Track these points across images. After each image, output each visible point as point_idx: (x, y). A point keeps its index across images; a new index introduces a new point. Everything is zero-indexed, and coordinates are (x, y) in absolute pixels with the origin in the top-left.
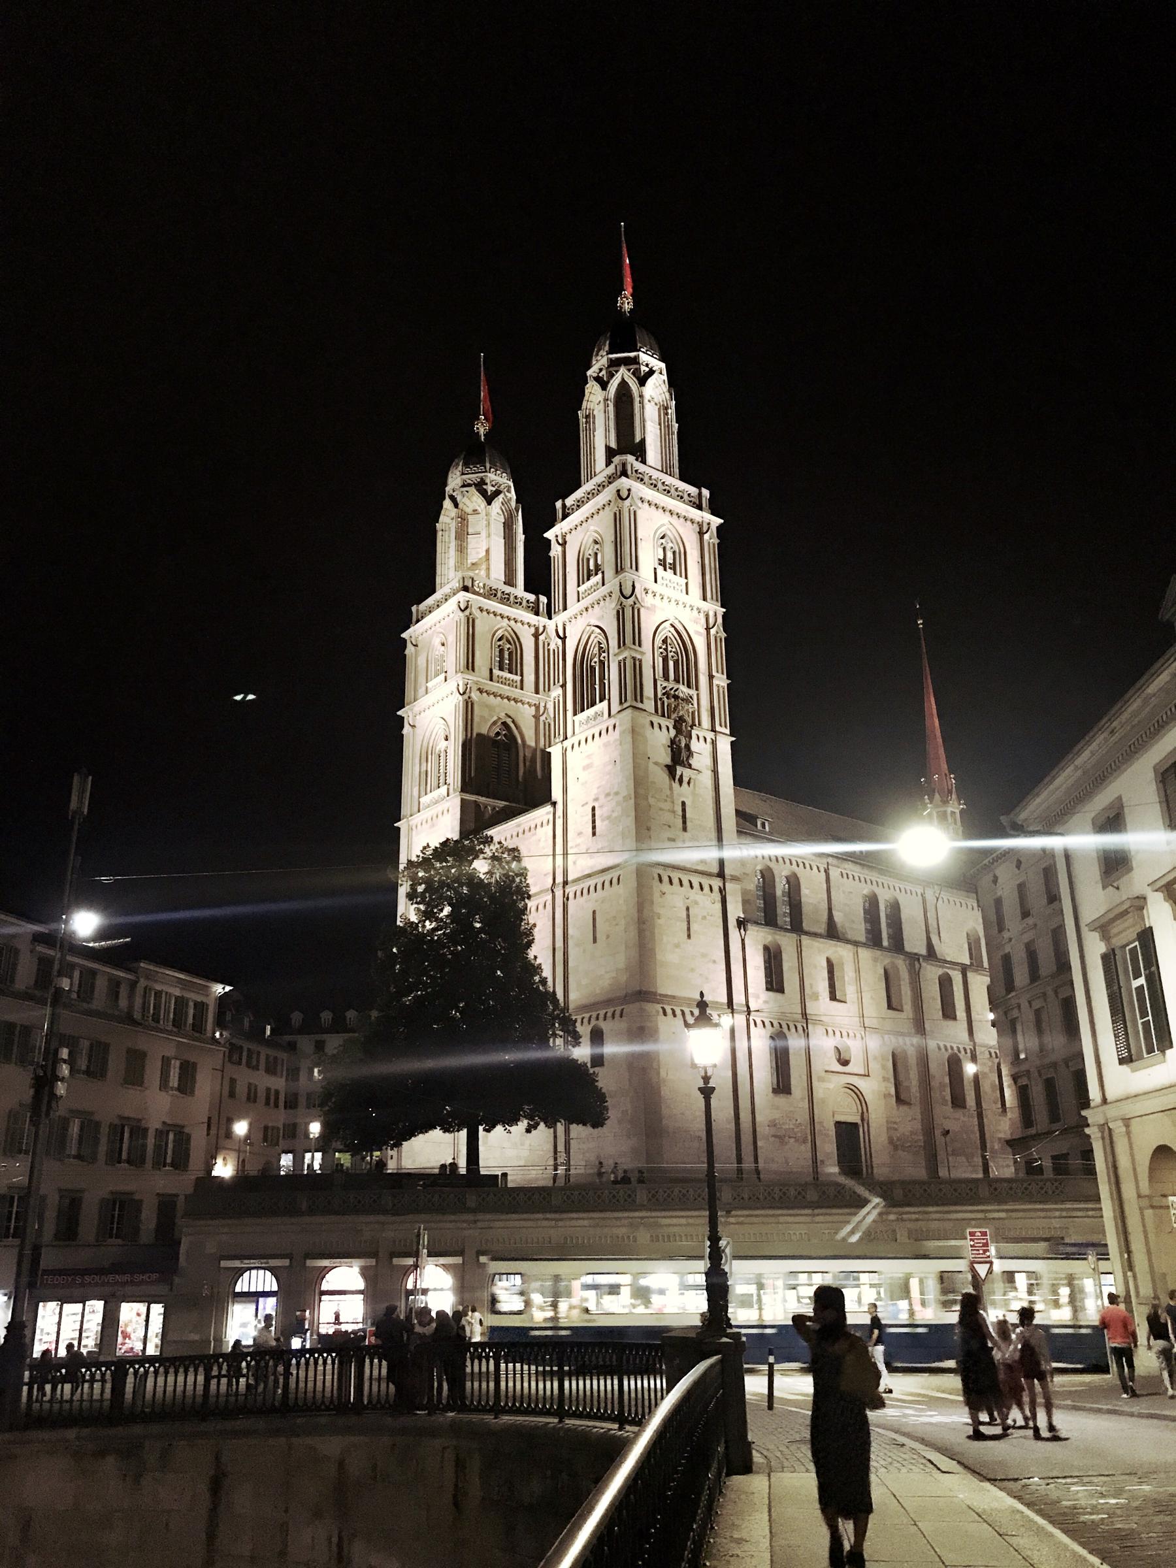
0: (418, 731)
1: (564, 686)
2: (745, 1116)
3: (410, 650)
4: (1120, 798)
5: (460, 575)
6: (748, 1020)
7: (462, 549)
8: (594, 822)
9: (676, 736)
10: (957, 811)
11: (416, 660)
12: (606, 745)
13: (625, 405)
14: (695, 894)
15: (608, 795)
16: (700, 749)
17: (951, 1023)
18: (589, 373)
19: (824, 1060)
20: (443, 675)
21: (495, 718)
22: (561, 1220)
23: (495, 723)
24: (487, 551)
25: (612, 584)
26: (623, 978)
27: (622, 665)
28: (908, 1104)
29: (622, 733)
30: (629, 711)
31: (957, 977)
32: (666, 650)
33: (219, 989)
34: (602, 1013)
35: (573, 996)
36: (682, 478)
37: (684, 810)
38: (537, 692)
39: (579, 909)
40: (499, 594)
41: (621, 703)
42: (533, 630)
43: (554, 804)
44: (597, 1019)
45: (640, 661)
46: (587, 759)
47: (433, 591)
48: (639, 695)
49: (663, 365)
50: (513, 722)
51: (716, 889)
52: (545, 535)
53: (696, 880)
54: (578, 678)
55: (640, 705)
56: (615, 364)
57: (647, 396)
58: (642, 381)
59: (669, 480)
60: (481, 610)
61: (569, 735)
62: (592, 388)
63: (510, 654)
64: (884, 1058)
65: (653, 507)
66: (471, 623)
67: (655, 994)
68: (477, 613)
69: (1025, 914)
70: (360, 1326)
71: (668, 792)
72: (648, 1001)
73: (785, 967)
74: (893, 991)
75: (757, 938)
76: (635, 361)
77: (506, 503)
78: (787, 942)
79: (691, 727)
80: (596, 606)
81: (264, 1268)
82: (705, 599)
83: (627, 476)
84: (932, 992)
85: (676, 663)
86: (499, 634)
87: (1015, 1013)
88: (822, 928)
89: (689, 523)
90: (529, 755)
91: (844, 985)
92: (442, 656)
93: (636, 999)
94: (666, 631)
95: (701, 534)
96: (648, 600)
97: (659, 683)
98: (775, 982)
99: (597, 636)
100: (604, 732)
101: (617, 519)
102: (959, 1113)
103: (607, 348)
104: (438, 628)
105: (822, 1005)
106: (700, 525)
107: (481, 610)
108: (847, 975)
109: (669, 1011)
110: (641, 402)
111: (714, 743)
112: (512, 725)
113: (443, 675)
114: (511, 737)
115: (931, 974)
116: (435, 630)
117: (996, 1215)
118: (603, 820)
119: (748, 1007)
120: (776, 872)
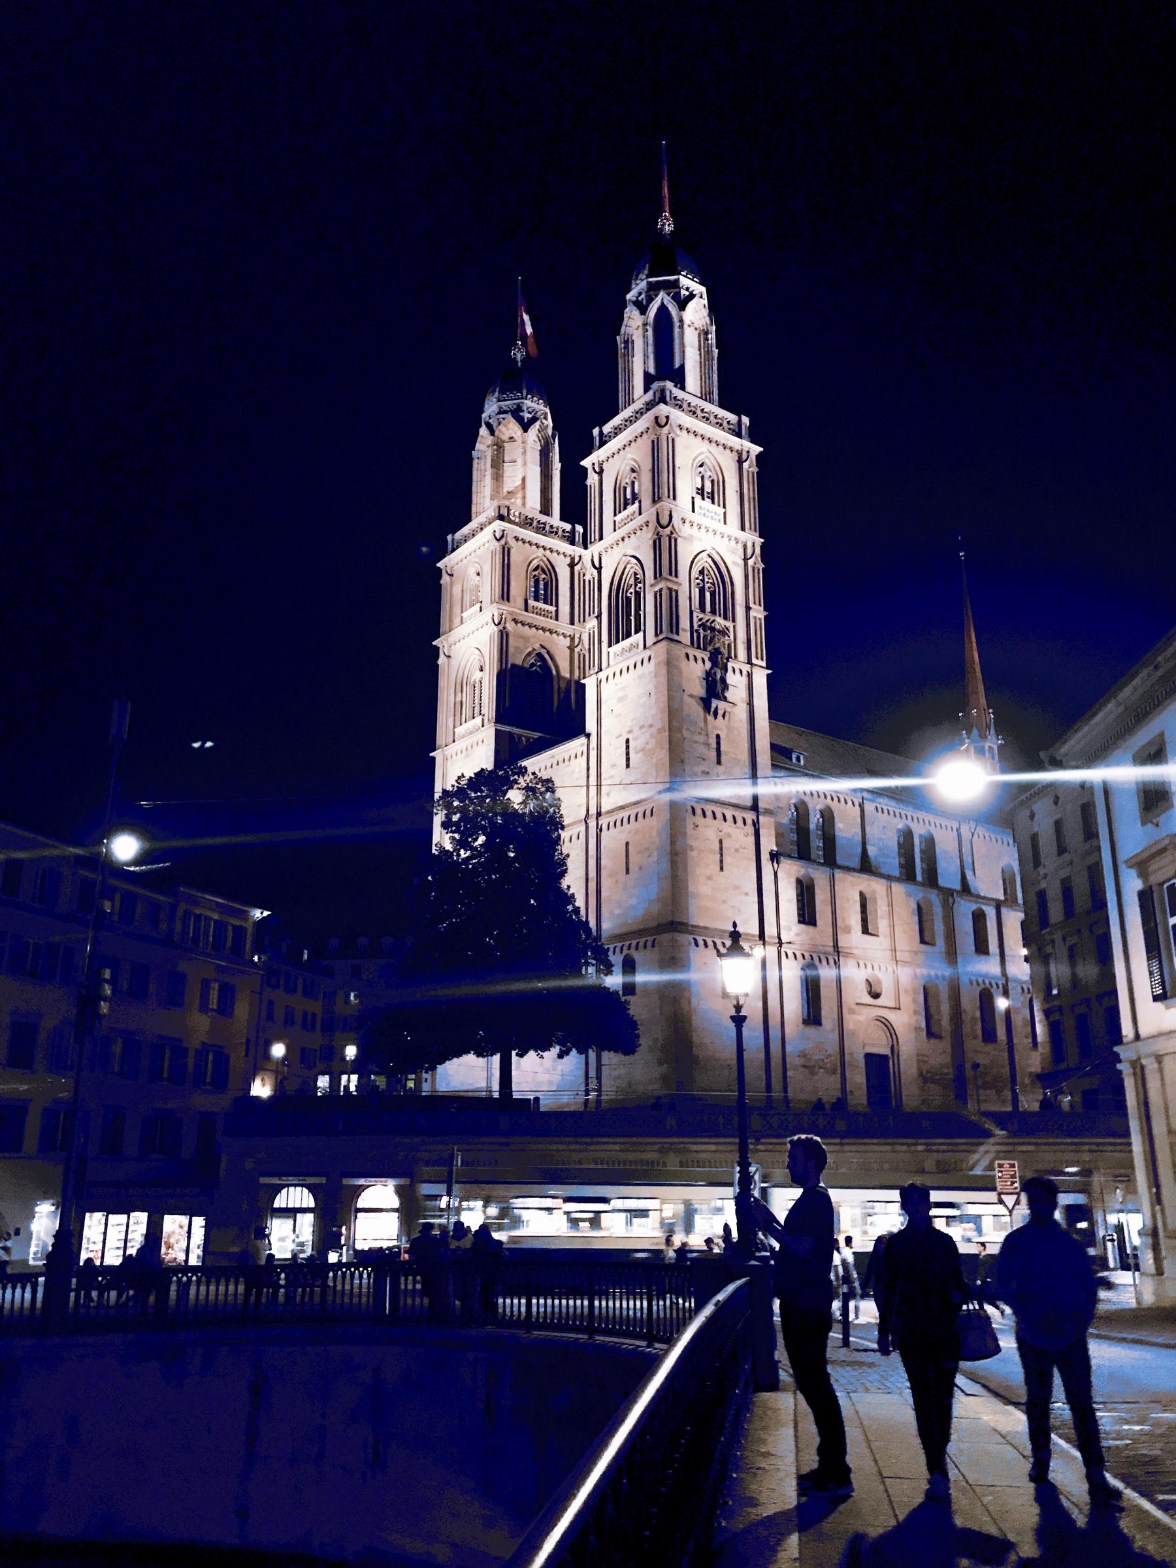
0: (453, 661)
1: (599, 617)
2: (775, 1046)
3: (445, 579)
4: (1162, 735)
5: (496, 503)
6: (779, 953)
7: (498, 477)
8: (628, 754)
9: (712, 668)
10: (995, 747)
11: (452, 590)
12: (641, 677)
14: (728, 827)
15: (642, 727)
17: (983, 957)
18: (628, 297)
19: (856, 993)
20: (477, 606)
21: (530, 649)
22: (591, 1144)
23: (529, 654)
24: (524, 479)
25: (649, 513)
26: (656, 908)
27: (658, 596)
28: (939, 1037)
29: (658, 664)
30: (664, 644)
31: (990, 912)
32: (703, 580)
33: (258, 914)
34: (634, 943)
35: (604, 926)
36: (722, 405)
37: (718, 743)
38: (572, 623)
39: (613, 840)
40: (535, 523)
41: (656, 635)
42: (568, 560)
43: (588, 736)
44: (629, 947)
45: (677, 592)
46: (623, 691)
47: (468, 520)
48: (674, 626)
49: (703, 289)
50: (548, 652)
51: (749, 822)
52: (582, 463)
53: (729, 813)
55: (676, 637)
56: (653, 289)
57: (687, 321)
58: (682, 304)
59: (708, 407)
60: (517, 539)
61: (604, 666)
63: (546, 585)
64: (915, 991)
65: (692, 435)
66: (506, 552)
67: (685, 925)
68: (512, 542)
69: (1062, 850)
70: (395, 1243)
71: (702, 725)
72: (681, 932)
73: (818, 902)
74: (926, 925)
75: (789, 872)
76: (676, 284)
77: (543, 429)
78: (820, 877)
79: (728, 660)
80: (632, 536)
81: (302, 1186)
82: (743, 529)
83: (666, 403)
84: (965, 926)
85: (713, 594)
86: (535, 564)
87: (1049, 949)
88: (856, 862)
89: (728, 451)
90: (563, 685)
91: (876, 918)
92: (477, 586)
93: (668, 929)
94: (703, 561)
95: (740, 462)
96: (685, 530)
97: (695, 615)
98: (807, 916)
99: (633, 566)
100: (639, 664)
101: (655, 447)
102: (989, 1048)
103: (646, 272)
104: (473, 558)
105: (853, 938)
106: (740, 453)
107: (517, 539)
108: (880, 908)
109: (701, 943)
110: (681, 327)
111: (750, 675)
112: (547, 656)
113: (477, 606)
114: (545, 667)
115: (964, 910)
116: (471, 560)
117: (1024, 1148)
118: (637, 753)
119: (780, 939)
120: (810, 806)
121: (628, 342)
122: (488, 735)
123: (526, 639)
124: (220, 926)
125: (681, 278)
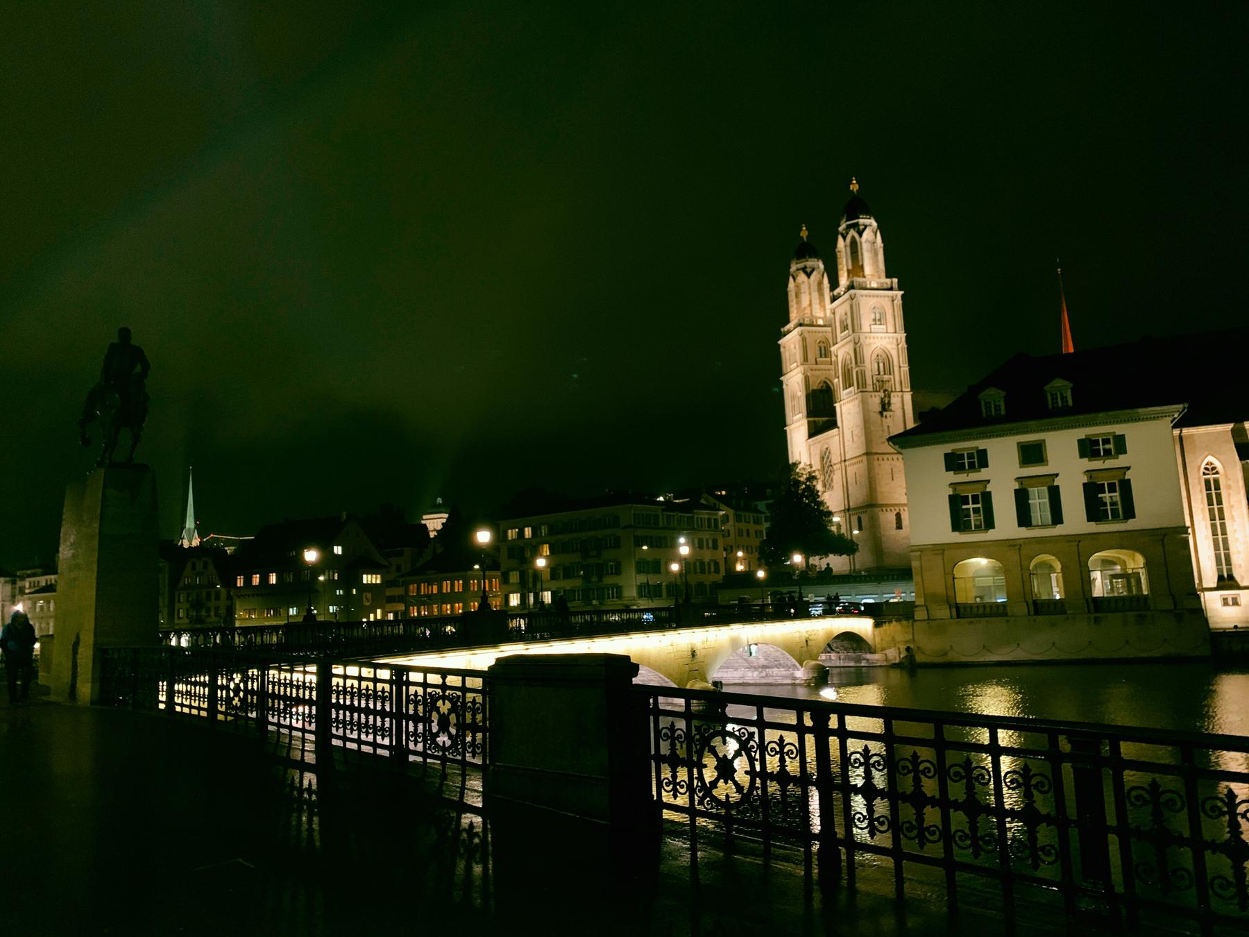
7: (799, 302)
13: (854, 248)
14: (895, 463)
16: (895, 400)
39: (851, 471)
46: (848, 408)
47: (788, 322)
48: (865, 385)
56: (849, 227)
58: (861, 235)
68: (806, 335)
76: (857, 225)
94: (878, 351)
96: (868, 341)
101: (851, 306)
116: (791, 343)
122: (805, 422)
123: (817, 376)
124: (709, 520)
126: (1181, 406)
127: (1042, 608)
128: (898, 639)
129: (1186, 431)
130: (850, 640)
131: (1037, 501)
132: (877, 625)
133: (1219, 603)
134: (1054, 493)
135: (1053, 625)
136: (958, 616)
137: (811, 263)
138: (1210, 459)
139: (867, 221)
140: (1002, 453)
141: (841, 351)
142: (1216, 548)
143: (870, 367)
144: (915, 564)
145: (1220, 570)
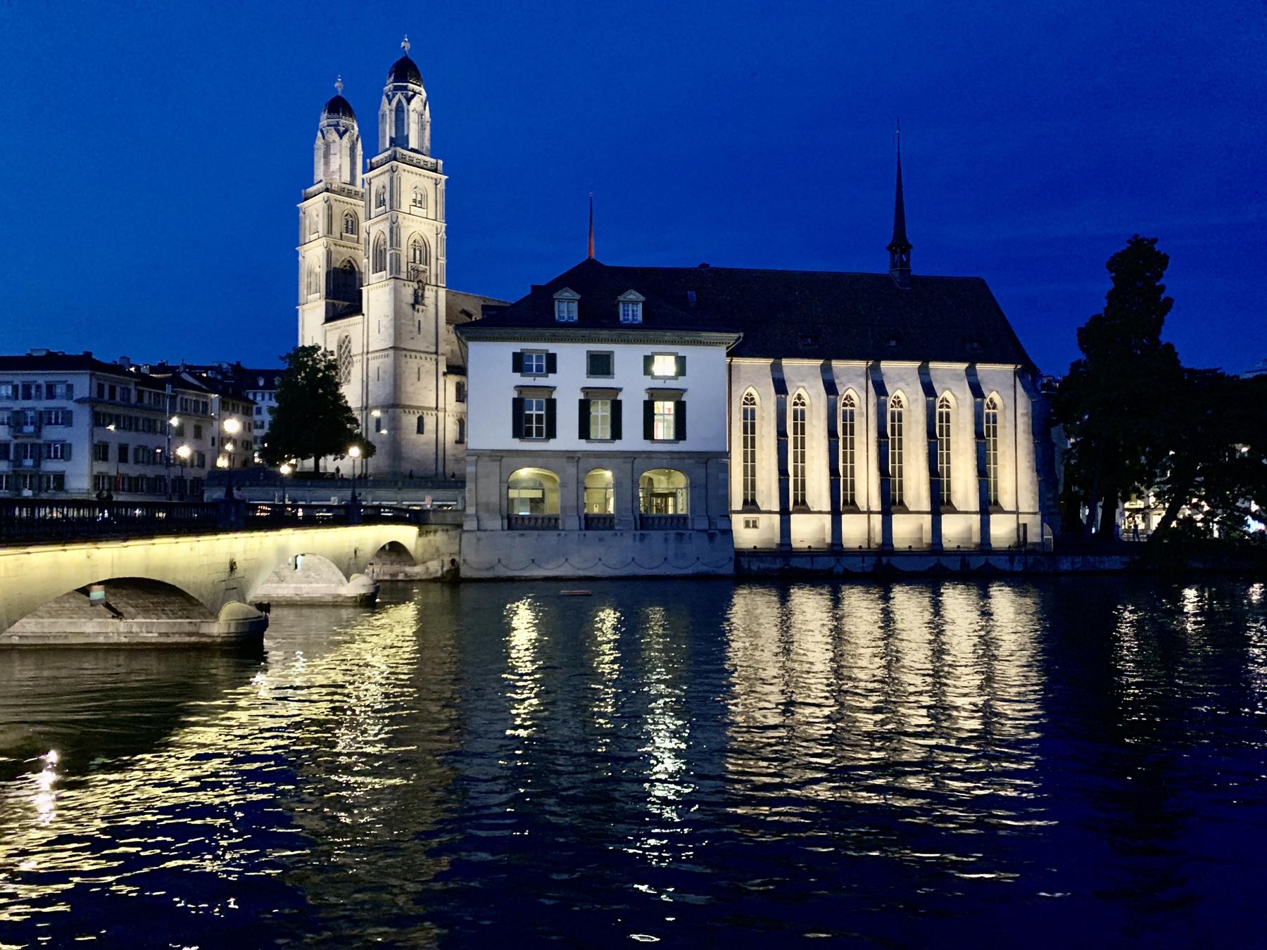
0: (307, 259)
2: (440, 453)
3: (301, 214)
7: (327, 163)
13: (400, 112)
14: (423, 362)
16: (429, 294)
39: (374, 364)
46: (378, 295)
48: (399, 270)
54: (375, 256)
56: (396, 88)
58: (409, 100)
62: (384, 99)
66: (330, 208)
68: (333, 202)
75: (452, 381)
76: (405, 88)
96: (406, 223)
114: (352, 267)
121: (384, 115)
122: (323, 303)
125: (411, 86)
126: (735, 336)
127: (592, 523)
128: (443, 550)
129: (735, 360)
130: (395, 549)
131: (600, 414)
132: (420, 535)
133: (742, 524)
134: (617, 408)
135: (601, 540)
136: (510, 528)
137: (345, 121)
138: (751, 390)
139: (417, 88)
140: (572, 358)
141: (374, 228)
142: (745, 474)
143: (406, 252)
144: (470, 470)
145: (745, 495)
